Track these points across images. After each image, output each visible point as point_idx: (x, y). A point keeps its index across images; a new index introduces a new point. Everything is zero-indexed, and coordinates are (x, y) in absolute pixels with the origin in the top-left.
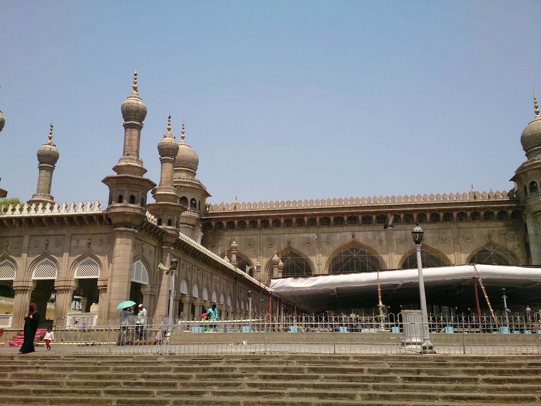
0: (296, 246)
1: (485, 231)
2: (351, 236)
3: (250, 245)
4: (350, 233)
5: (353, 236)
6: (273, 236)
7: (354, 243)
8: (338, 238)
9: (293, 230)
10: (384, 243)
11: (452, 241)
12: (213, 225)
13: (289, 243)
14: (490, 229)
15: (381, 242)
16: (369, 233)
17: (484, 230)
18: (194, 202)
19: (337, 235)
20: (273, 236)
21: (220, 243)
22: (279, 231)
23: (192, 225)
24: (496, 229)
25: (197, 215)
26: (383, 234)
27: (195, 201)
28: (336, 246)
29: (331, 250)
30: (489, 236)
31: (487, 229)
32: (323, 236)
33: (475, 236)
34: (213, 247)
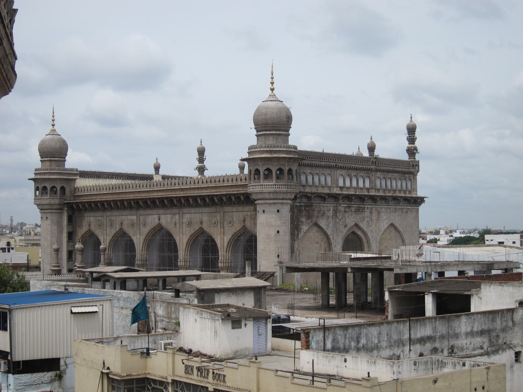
0: (126, 228)
1: (241, 215)
3: (100, 225)
4: (156, 216)
5: (159, 219)
6: (113, 218)
9: (123, 212)
10: (178, 226)
11: (219, 225)
13: (122, 224)
14: (245, 213)
16: (169, 216)
17: (241, 214)
18: (55, 189)
19: (150, 217)
20: (113, 218)
21: (84, 224)
22: (116, 213)
23: (56, 209)
24: (249, 213)
25: (57, 201)
29: (145, 231)
31: (243, 213)
33: (235, 220)
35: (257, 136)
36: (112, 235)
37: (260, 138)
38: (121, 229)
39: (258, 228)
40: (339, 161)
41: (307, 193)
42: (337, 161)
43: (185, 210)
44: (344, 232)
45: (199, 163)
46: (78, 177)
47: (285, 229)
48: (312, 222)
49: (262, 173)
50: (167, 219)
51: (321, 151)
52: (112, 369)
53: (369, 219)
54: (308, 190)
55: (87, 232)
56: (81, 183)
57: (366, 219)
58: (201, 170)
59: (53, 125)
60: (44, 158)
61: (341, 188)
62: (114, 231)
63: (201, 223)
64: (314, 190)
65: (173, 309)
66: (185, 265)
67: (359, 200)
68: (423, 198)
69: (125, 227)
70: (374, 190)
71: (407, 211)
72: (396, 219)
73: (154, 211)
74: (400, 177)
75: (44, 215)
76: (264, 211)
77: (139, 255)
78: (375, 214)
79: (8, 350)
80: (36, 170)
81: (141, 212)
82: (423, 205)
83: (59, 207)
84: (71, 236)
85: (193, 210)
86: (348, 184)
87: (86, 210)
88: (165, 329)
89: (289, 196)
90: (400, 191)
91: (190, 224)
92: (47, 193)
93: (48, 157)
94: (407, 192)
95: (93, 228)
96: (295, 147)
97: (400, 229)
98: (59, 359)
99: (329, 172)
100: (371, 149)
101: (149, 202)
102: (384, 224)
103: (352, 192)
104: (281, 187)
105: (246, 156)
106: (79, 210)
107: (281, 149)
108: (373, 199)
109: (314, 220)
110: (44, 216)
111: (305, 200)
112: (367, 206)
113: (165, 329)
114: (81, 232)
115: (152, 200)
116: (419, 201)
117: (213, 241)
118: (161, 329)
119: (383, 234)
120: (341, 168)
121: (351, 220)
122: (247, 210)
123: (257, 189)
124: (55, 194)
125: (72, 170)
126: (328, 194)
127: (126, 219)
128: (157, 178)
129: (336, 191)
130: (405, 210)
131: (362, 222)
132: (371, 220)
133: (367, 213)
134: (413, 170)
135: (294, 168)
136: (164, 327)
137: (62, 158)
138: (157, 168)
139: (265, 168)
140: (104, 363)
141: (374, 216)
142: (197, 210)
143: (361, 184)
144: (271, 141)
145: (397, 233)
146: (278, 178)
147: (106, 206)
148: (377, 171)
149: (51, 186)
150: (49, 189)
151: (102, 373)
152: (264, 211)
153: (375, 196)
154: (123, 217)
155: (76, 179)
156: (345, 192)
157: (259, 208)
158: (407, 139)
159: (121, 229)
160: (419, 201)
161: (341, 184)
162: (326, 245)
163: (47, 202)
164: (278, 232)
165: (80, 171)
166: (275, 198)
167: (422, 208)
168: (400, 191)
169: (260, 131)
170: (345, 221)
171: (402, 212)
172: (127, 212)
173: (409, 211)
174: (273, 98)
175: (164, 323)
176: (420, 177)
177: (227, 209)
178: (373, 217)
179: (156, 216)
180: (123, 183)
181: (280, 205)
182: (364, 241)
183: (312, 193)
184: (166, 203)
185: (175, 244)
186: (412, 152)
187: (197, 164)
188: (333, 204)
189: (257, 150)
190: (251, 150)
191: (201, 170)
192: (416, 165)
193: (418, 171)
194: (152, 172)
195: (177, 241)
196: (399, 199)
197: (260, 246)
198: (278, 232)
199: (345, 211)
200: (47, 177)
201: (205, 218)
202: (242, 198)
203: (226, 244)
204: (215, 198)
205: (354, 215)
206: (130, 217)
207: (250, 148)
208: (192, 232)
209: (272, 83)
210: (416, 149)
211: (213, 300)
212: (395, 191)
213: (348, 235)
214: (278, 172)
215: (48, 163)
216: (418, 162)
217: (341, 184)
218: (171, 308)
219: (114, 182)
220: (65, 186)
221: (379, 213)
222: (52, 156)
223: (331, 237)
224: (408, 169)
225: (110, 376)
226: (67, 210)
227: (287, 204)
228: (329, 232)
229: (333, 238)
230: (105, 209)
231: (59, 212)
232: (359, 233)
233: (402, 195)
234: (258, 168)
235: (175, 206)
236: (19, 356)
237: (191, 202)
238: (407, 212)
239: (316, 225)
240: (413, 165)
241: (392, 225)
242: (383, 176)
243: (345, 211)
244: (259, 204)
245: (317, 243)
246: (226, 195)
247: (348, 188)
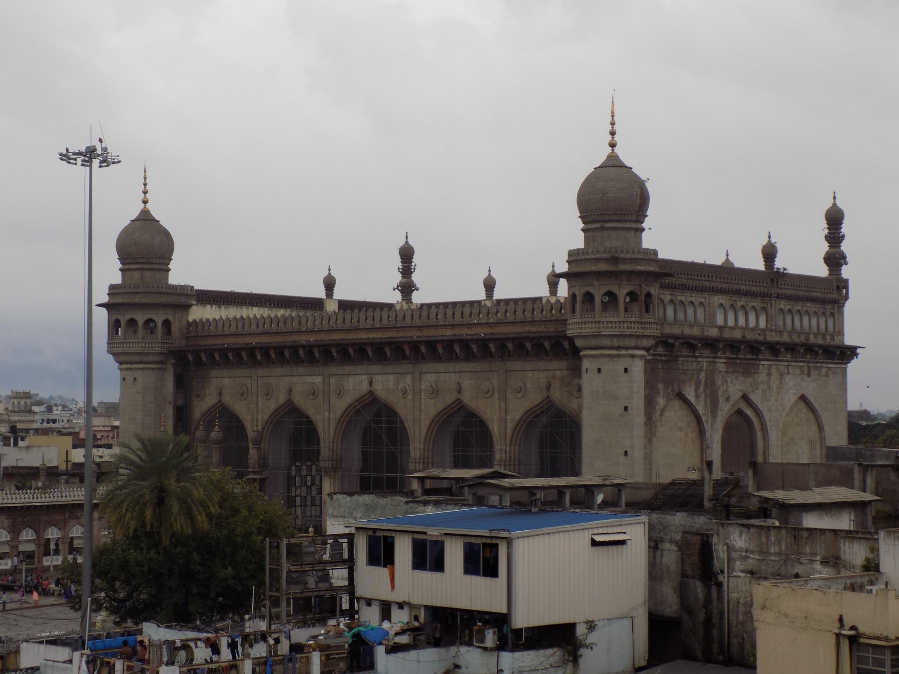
2: (367, 382)
3: (243, 394)
4: (364, 377)
5: (371, 383)
6: (272, 381)
7: (371, 391)
8: (351, 385)
10: (409, 397)
11: (496, 395)
12: (191, 359)
13: (290, 390)
15: (405, 393)
16: (391, 377)
18: (151, 325)
19: (350, 380)
20: (272, 381)
21: (208, 392)
22: (278, 371)
23: (155, 363)
24: (558, 373)
25: (157, 348)
26: (409, 379)
28: (348, 400)
29: (340, 405)
30: (548, 387)
32: (333, 380)
33: (529, 385)
34: (198, 396)
35: (583, 230)
36: (270, 412)
37: (589, 234)
38: (289, 402)
39: (587, 401)
40: (718, 280)
41: (667, 338)
42: (714, 279)
43: (426, 367)
44: (725, 410)
45: (403, 277)
46: (194, 302)
47: (638, 404)
48: (673, 391)
49: (598, 301)
50: (386, 383)
51: (717, 260)
52: (862, 629)
53: (765, 387)
54: (667, 330)
55: (214, 406)
56: (199, 313)
57: (761, 387)
58: (407, 288)
59: (145, 202)
60: (129, 264)
61: (720, 328)
62: (273, 406)
63: (459, 392)
64: (677, 331)
65: (772, 538)
67: (747, 351)
68: (856, 348)
69: (297, 398)
70: (774, 334)
71: (827, 373)
72: (810, 387)
73: (360, 368)
74: (816, 310)
75: (126, 373)
76: (599, 370)
77: (327, 451)
78: (775, 376)
79: (500, 607)
80: (112, 287)
81: (333, 369)
82: (854, 361)
83: (160, 358)
84: (182, 415)
85: (441, 367)
86: (731, 322)
87: (214, 364)
88: (752, 573)
89: (645, 343)
90: (816, 335)
91: (435, 392)
92: (135, 332)
93: (136, 263)
94: (828, 337)
95: (227, 399)
96: (655, 252)
97: (816, 405)
98: (572, 627)
99: (702, 300)
100: (769, 253)
101: (351, 351)
102: (791, 397)
103: (738, 335)
104: (633, 325)
105: (563, 267)
106: (199, 362)
107: (634, 256)
108: (774, 349)
109: (676, 388)
110: (129, 375)
111: (660, 350)
112: (762, 362)
113: (752, 573)
114: (201, 407)
115: (357, 348)
116: (850, 353)
117: (482, 424)
118: (742, 571)
119: (788, 415)
120: (721, 291)
121: (733, 387)
122: (558, 368)
123: (588, 329)
124: (152, 333)
125: (184, 287)
126: (700, 339)
127: (301, 385)
128: (331, 307)
129: (713, 333)
130: (824, 370)
131: (753, 392)
132: (769, 388)
133: (762, 377)
134: (835, 296)
135: (654, 291)
136: (750, 568)
137: (163, 264)
138: (329, 284)
139: (604, 290)
140: (841, 620)
141: (774, 384)
142: (451, 366)
143: (749, 321)
144: (614, 241)
145: (810, 414)
146: (626, 310)
147: (259, 358)
148: (779, 297)
149: (146, 317)
150: (140, 323)
151: (838, 635)
152: (599, 370)
153: (778, 343)
154: (295, 379)
155: (192, 305)
156: (727, 334)
157: (586, 364)
158: (826, 237)
159: (289, 402)
160: (849, 353)
161: (720, 321)
162: (694, 435)
163: (137, 349)
164: (626, 408)
165: (196, 290)
166: (620, 345)
167: (853, 367)
168: (816, 335)
169: (594, 222)
170: (726, 390)
171: (819, 375)
172: (301, 370)
173: (830, 372)
174: (613, 164)
175: (751, 561)
176: (849, 308)
177: (513, 365)
178: (772, 383)
179: (364, 378)
180: (294, 314)
181: (630, 359)
182: (757, 426)
183: (676, 337)
184: (388, 353)
185: (404, 429)
186: (835, 260)
187: (398, 278)
188: (709, 357)
189: (588, 257)
190: (574, 257)
191: (407, 288)
192: (844, 288)
193: (846, 297)
194: (319, 292)
195: (409, 425)
196: (816, 349)
197: (588, 436)
198: (626, 408)
199: (727, 372)
200: (137, 299)
201: (467, 383)
202: (547, 345)
203: (509, 431)
204: (492, 346)
205: (742, 379)
206: (309, 379)
207: (571, 253)
208: (441, 407)
209: (613, 133)
210: (844, 257)
211: (801, 523)
212: (808, 334)
213: (730, 417)
214: (628, 300)
215: (137, 274)
216: (847, 281)
217: (720, 321)
218: (768, 537)
219: (256, 312)
220: (170, 318)
221: (782, 376)
222: (145, 260)
223: (704, 419)
224: (830, 293)
225: (862, 640)
227: (641, 357)
228: (701, 411)
229: (707, 422)
230: (254, 363)
231: (159, 369)
232: (749, 412)
233: (820, 341)
234: (592, 291)
235: (405, 357)
236: (522, 620)
237: (441, 351)
238: (827, 375)
239: (681, 397)
240: (838, 287)
241: (803, 398)
242: (788, 307)
243: (727, 372)
244: (585, 356)
245: (681, 429)
246: (512, 340)
247: (733, 328)
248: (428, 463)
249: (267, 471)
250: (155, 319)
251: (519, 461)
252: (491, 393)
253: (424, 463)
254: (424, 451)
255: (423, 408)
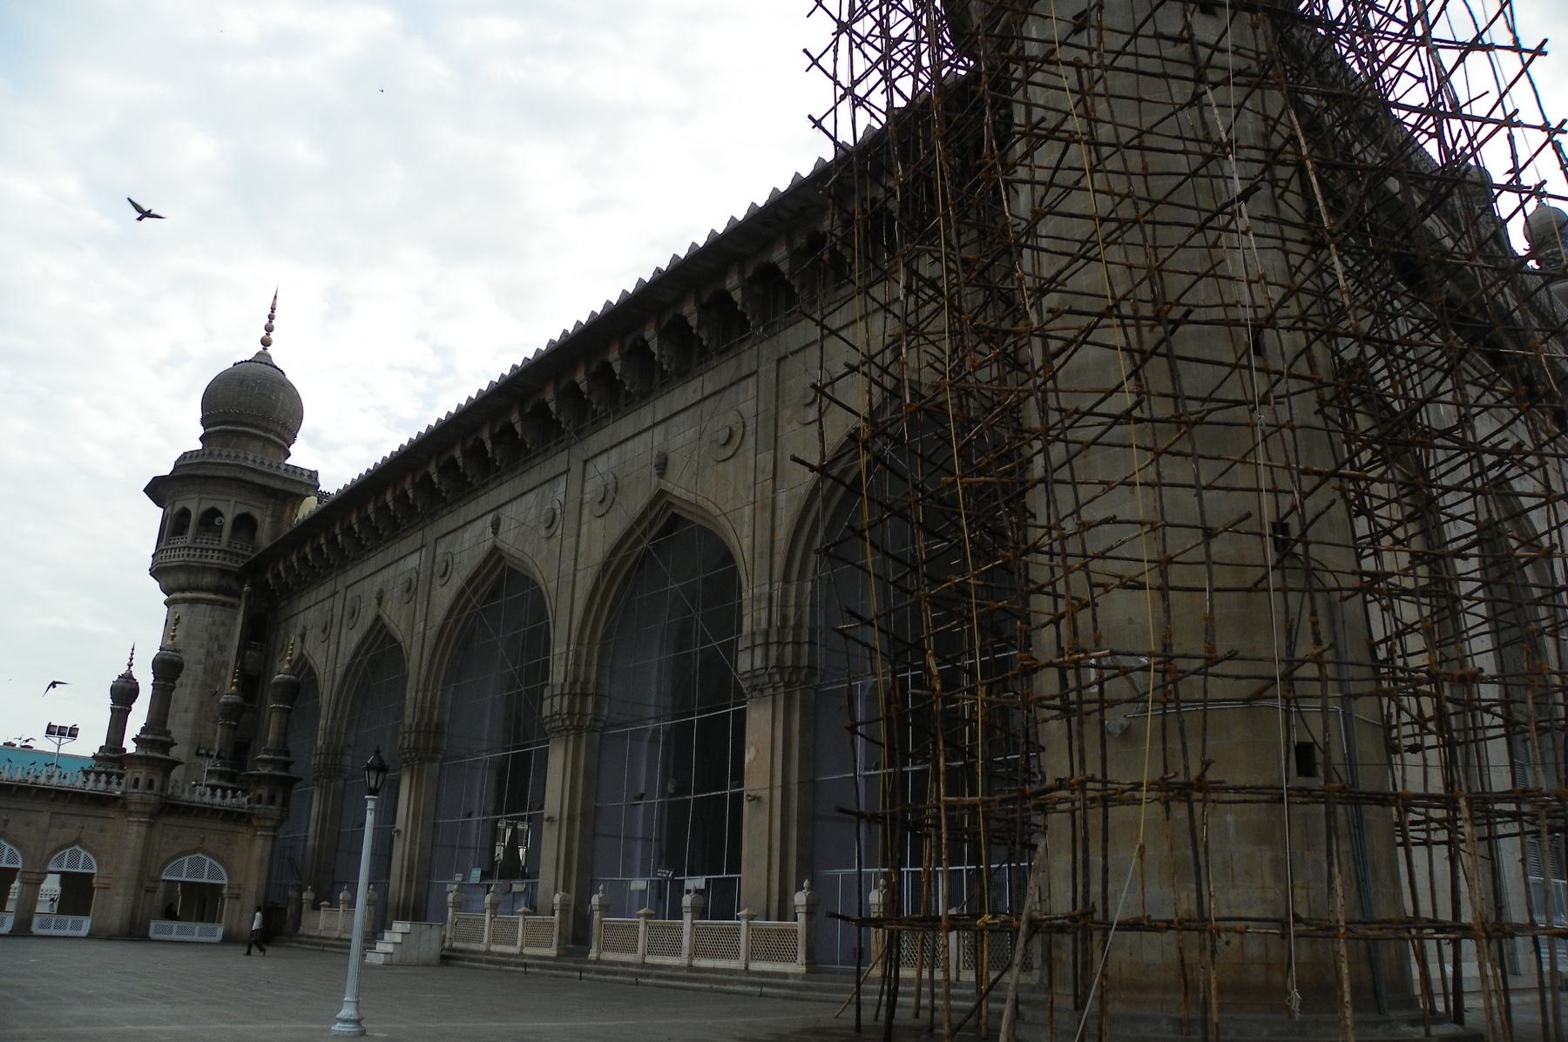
23: (216, 592)
25: (214, 560)
27: (220, 514)
59: (266, 343)
66: (570, 713)
149: (206, 506)
203: (783, 533)
220: (257, 514)
226: (249, 595)
231: (224, 604)
248: (584, 695)
249: (341, 783)
250: (222, 507)
251: (812, 631)
252: (737, 439)
253: (572, 695)
254: (577, 664)
255: (582, 548)
